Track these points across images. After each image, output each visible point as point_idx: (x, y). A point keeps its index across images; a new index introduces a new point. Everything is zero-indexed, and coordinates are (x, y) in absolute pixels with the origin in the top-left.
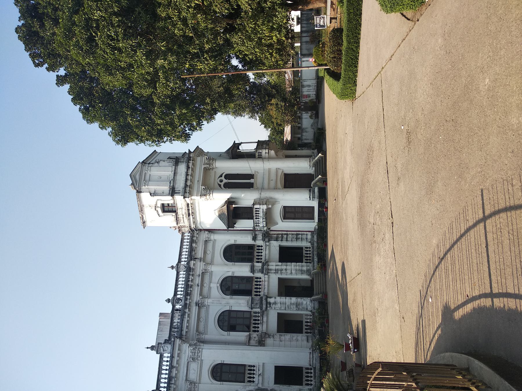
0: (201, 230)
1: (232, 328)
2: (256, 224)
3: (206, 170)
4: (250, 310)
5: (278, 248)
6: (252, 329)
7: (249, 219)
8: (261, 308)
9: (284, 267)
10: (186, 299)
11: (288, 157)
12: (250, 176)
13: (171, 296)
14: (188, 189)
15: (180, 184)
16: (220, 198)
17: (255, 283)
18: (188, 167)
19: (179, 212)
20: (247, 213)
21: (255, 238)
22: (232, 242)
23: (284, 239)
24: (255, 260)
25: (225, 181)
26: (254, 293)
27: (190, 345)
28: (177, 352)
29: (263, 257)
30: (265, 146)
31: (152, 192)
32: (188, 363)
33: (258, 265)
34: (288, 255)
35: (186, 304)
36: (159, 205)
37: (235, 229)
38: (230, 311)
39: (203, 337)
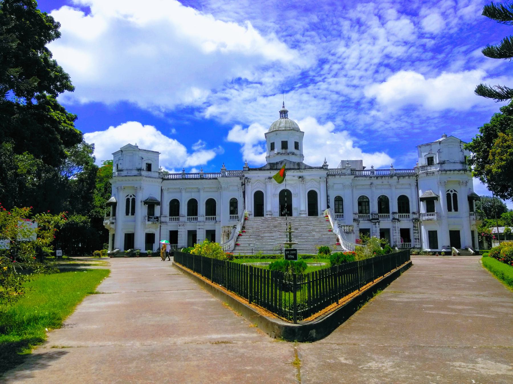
1: (360, 204)
2: (424, 215)
6: (360, 215)
7: (427, 209)
8: (373, 219)
9: (397, 231)
10: (374, 177)
12: (456, 209)
13: (375, 168)
14: (444, 172)
15: (446, 167)
17: (386, 214)
18: (459, 170)
19: (429, 168)
23: (415, 231)
24: (400, 214)
25: (452, 194)
26: (380, 214)
27: (351, 184)
29: (402, 219)
30: (479, 217)
31: (441, 151)
33: (397, 216)
34: (405, 234)
35: (371, 177)
38: (368, 202)
39: (354, 189)
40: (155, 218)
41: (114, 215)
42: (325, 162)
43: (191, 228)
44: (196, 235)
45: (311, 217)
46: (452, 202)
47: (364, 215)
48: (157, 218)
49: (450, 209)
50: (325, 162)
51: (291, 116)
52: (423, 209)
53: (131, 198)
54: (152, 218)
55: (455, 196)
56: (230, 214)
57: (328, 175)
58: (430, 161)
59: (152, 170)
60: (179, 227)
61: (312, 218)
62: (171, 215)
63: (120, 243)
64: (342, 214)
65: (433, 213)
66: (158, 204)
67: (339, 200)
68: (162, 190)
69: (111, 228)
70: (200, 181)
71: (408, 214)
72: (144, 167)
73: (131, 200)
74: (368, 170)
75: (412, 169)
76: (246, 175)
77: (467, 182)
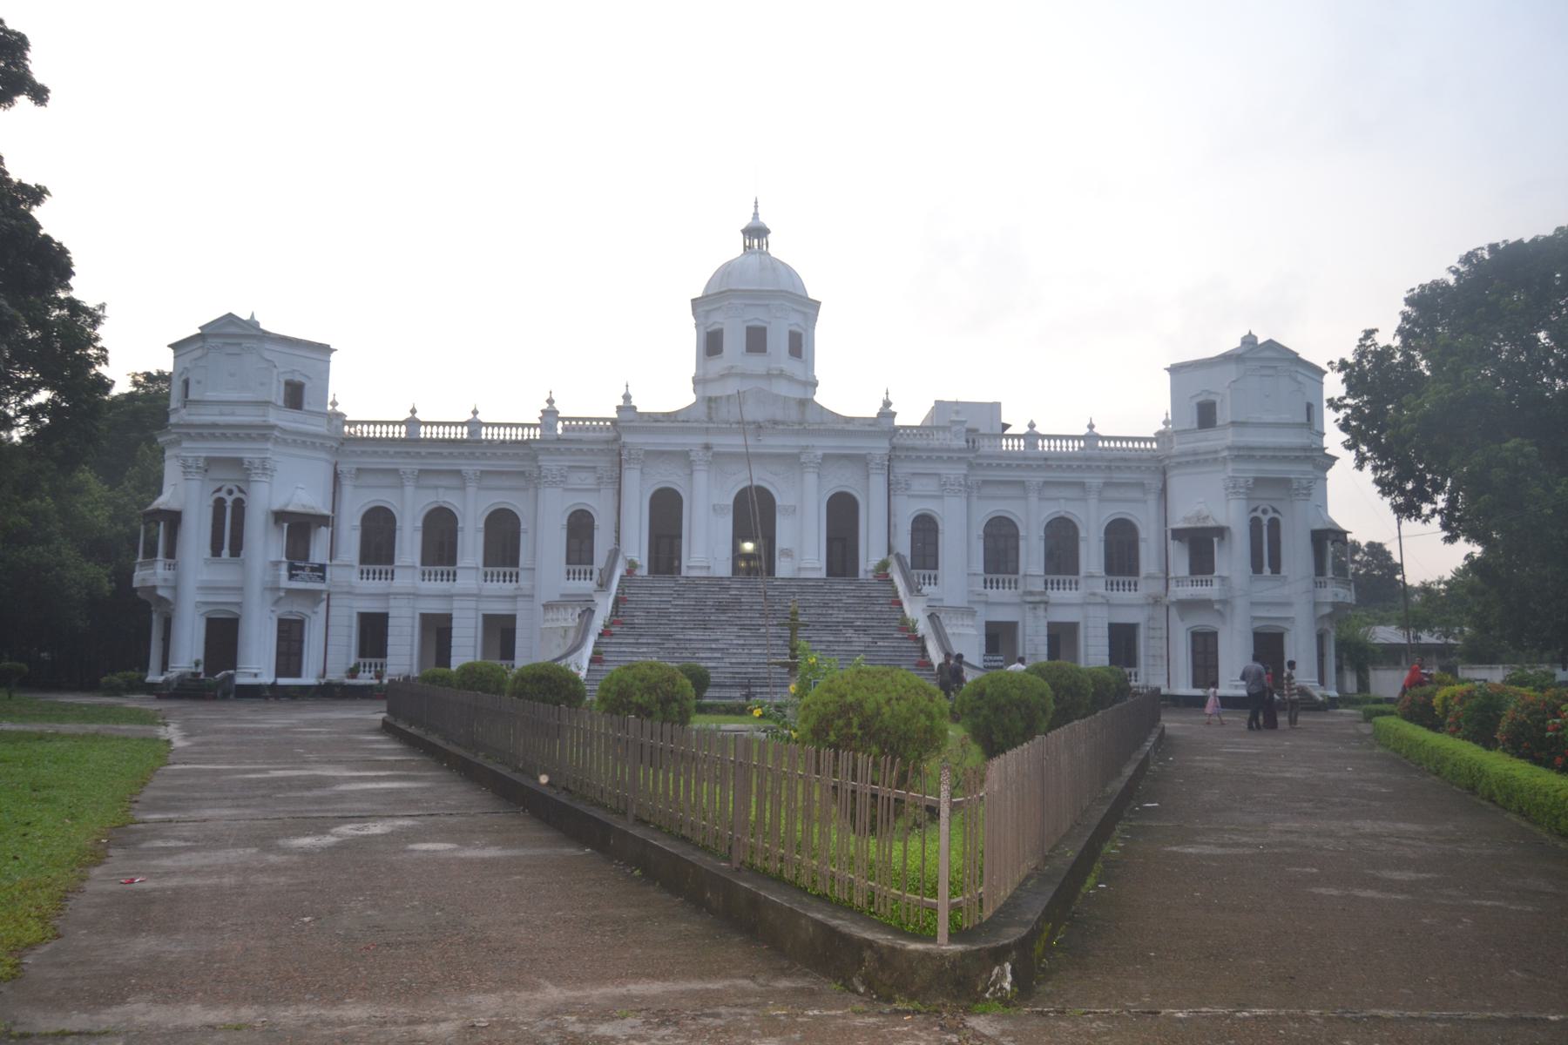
0: (1165, 473)
2: (1179, 581)
3: (1283, 483)
4: (1021, 572)
5: (1132, 621)
6: (989, 577)
11: (1321, 638)
12: (1276, 567)
13: (1039, 429)
16: (1229, 513)
17: (1068, 578)
20: (1202, 563)
21: (1148, 577)
22: (1143, 534)
25: (1265, 519)
27: (966, 476)
28: (955, 455)
32: (938, 475)
34: (1123, 640)
36: (1212, 397)
37: (1170, 542)
38: (1016, 536)
40: (313, 569)
41: (171, 553)
42: (887, 404)
43: (435, 607)
44: (450, 629)
45: (837, 580)
46: (1266, 550)
47: (1001, 577)
48: (322, 568)
49: (1257, 567)
50: (887, 404)
51: (778, 247)
52: (1180, 562)
53: (229, 500)
54: (302, 568)
55: (1274, 525)
56: (568, 562)
57: (894, 448)
58: (1206, 415)
59: (306, 407)
60: (392, 602)
61: (840, 584)
62: (365, 558)
63: (188, 651)
64: (933, 573)
65: (1204, 577)
66: (323, 520)
67: (925, 528)
68: (337, 477)
69: (161, 599)
70: (467, 451)
71: (1132, 579)
72: (277, 394)
73: (229, 503)
74: (1019, 437)
75: (1151, 440)
76: (626, 438)
77: (1309, 488)
